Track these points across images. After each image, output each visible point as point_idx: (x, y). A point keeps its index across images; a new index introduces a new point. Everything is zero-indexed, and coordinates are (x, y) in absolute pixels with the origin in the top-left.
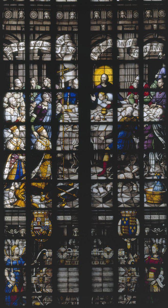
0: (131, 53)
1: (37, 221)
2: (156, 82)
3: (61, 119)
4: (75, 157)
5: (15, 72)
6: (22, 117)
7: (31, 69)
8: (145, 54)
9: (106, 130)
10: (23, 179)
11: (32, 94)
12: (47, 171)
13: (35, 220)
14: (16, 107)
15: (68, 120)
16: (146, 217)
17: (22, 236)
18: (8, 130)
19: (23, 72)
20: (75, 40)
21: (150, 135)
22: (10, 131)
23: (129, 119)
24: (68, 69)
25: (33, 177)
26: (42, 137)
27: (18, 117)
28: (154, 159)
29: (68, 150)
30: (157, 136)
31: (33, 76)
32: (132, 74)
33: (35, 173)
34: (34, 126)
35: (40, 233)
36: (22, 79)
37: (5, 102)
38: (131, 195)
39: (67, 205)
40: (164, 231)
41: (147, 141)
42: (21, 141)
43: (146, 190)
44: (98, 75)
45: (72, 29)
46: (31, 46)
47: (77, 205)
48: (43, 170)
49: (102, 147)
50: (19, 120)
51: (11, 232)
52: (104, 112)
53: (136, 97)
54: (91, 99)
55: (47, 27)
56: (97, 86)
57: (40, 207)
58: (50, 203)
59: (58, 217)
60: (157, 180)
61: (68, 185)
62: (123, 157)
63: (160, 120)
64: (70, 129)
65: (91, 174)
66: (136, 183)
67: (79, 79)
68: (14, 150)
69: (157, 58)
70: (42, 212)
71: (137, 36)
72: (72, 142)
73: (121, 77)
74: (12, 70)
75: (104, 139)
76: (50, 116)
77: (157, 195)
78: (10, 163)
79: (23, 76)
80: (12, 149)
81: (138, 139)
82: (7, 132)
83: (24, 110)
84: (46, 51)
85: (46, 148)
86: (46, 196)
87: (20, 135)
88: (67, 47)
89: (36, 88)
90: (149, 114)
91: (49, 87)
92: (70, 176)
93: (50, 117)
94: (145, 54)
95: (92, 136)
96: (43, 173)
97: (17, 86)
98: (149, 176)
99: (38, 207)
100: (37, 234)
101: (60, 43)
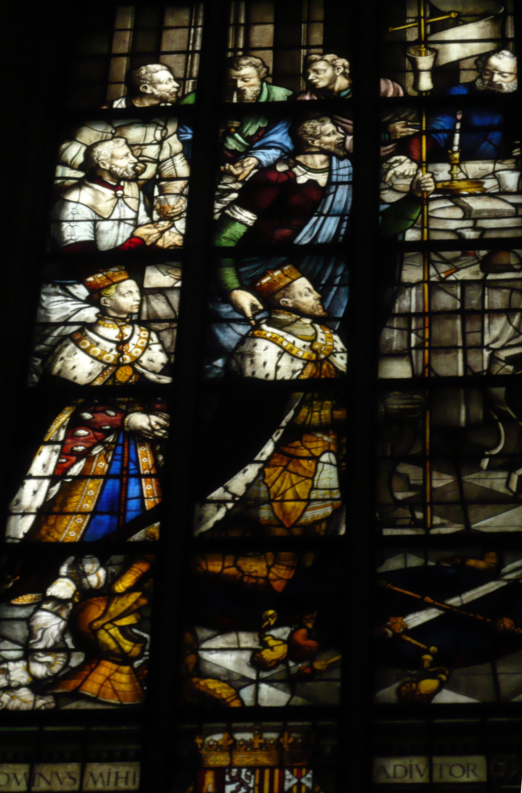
3: (412, 227)
6: (162, 223)
10: (139, 536)
12: (313, 488)
15: (454, 231)
18: (71, 289)
22: (81, 291)
25: (210, 524)
26: (283, 317)
27: (137, 226)
37: (65, 164)
39: (455, 688)
42: (149, 338)
50: (145, 238)
59: (380, 761)
68: (98, 383)
72: (482, 332)
74: (126, 30)
76: (341, 215)
78: (62, 454)
79: (186, 52)
83: (181, 194)
86: (303, 632)
87: (145, 308)
89: (259, 96)
91: (340, 91)
97: (149, 91)
99: (236, 704)
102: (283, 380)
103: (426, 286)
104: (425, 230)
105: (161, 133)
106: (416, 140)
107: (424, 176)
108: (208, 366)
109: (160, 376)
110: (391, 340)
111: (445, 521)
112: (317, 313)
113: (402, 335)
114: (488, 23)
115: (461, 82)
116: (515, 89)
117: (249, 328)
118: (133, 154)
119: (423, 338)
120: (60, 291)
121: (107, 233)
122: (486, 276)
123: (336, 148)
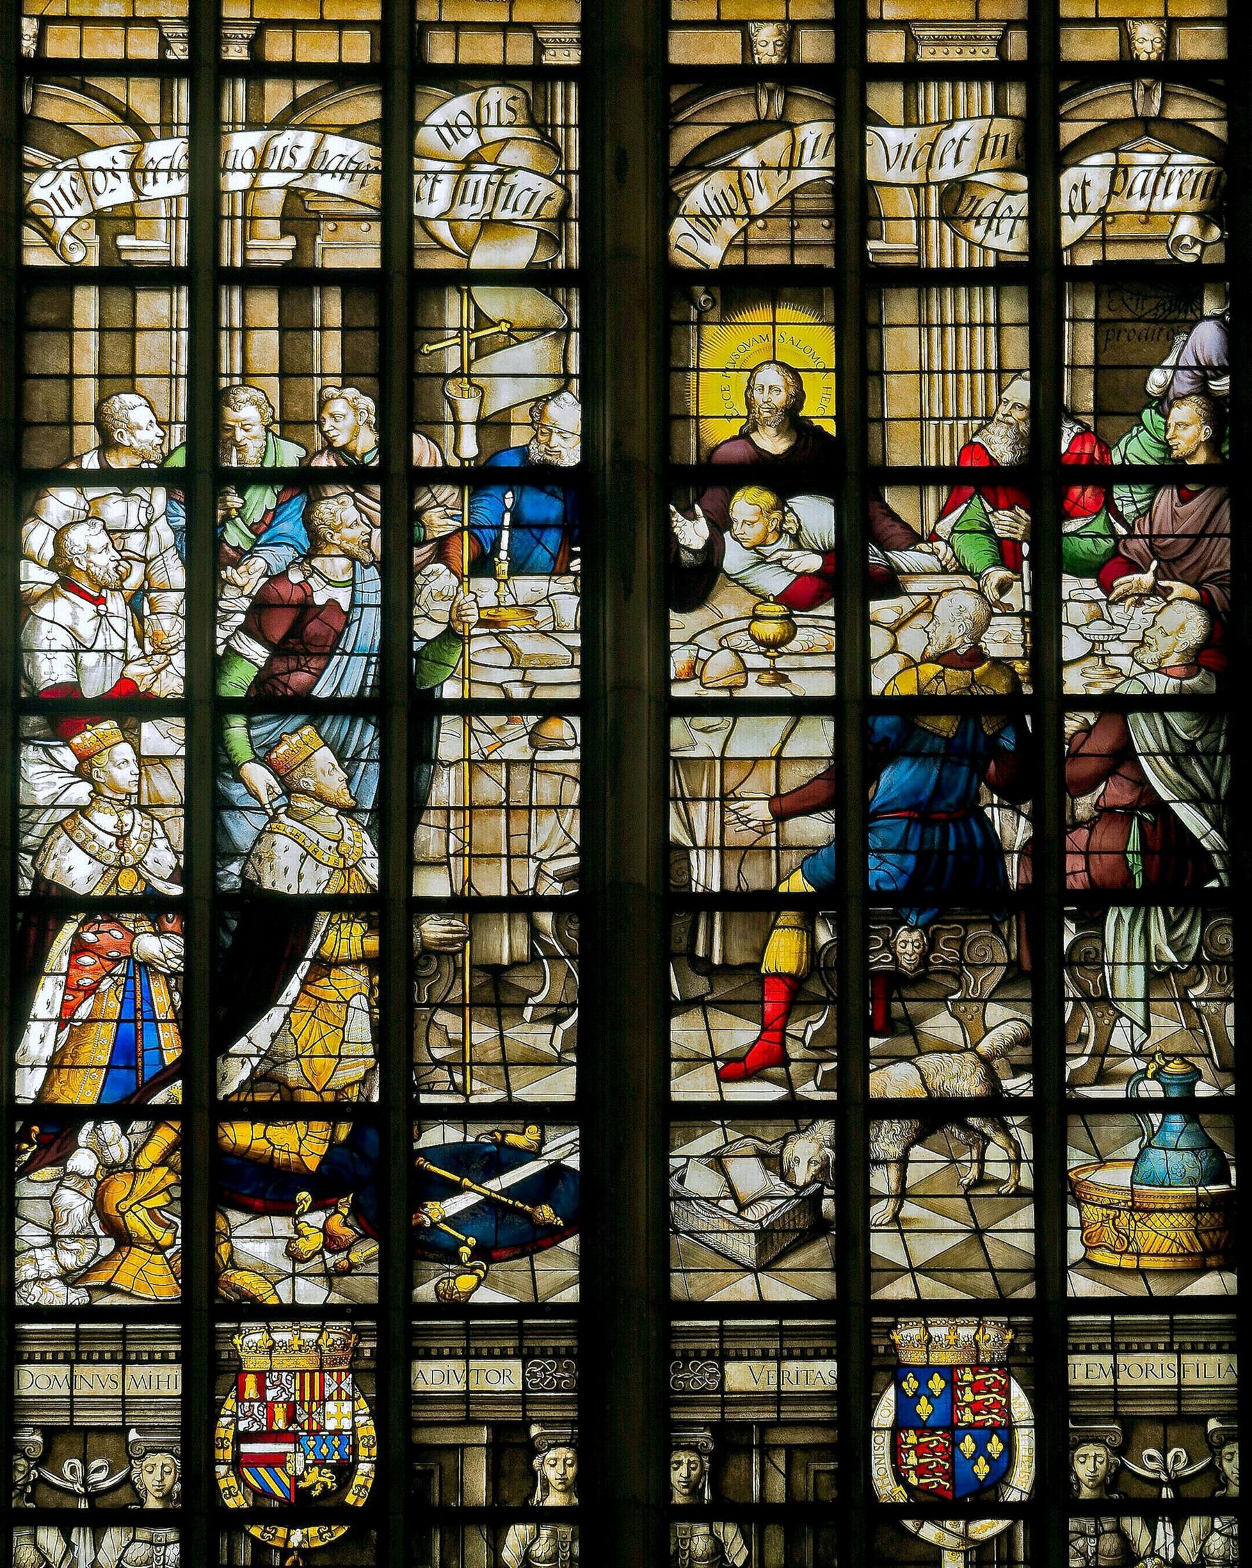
0: (967, 219)
1: (262, 1398)
2: (1157, 417)
4: (553, 942)
5: (108, 347)
6: (156, 657)
7: (231, 329)
10: (160, 1098)
12: (343, 1041)
13: (251, 1390)
15: (500, 685)
16: (1081, 1370)
17: (152, 1503)
19: (174, 348)
20: (554, 126)
21: (1115, 792)
22: (67, 757)
23: (955, 680)
24: (504, 327)
25: (234, 1086)
26: (304, 804)
28: (1138, 956)
29: (504, 893)
30: (1165, 794)
32: (979, 378)
33: (248, 1056)
34: (249, 726)
35: (287, 1482)
37: (30, 559)
38: (973, 1215)
39: (494, 1286)
40: (1213, 1471)
41: (1091, 830)
43: (1083, 1176)
45: (539, 47)
46: (234, 170)
47: (568, 1284)
49: (756, 877)
51: (68, 1475)
52: (769, 630)
54: (676, 536)
55: (349, 35)
56: (718, 447)
57: (287, 1300)
58: (362, 1270)
60: (1164, 1106)
61: (501, 1144)
62: (908, 943)
63: (1184, 682)
64: (517, 749)
65: (674, 1065)
66: (1005, 1129)
67: (585, 399)
68: (99, 892)
69: (1158, 253)
70: (305, 1336)
71: (1016, 100)
73: (892, 382)
75: (768, 816)
77: (1162, 1211)
78: (67, 988)
79: (170, 376)
80: (81, 889)
81: (1022, 819)
82: (46, 768)
87: (144, 787)
88: (496, 178)
90: (1102, 642)
91: (364, 455)
92: (512, 1077)
93: (369, 664)
95: (683, 799)
97: (126, 443)
98: (1103, 1078)
99: (273, 1301)
100: (262, 1493)
101: (448, 146)
103: (466, 764)
106: (456, 539)
107: (465, 599)
109: (170, 885)
110: (427, 842)
111: (485, 1086)
112: (343, 801)
115: (512, 446)
116: (578, 460)
122: (534, 754)
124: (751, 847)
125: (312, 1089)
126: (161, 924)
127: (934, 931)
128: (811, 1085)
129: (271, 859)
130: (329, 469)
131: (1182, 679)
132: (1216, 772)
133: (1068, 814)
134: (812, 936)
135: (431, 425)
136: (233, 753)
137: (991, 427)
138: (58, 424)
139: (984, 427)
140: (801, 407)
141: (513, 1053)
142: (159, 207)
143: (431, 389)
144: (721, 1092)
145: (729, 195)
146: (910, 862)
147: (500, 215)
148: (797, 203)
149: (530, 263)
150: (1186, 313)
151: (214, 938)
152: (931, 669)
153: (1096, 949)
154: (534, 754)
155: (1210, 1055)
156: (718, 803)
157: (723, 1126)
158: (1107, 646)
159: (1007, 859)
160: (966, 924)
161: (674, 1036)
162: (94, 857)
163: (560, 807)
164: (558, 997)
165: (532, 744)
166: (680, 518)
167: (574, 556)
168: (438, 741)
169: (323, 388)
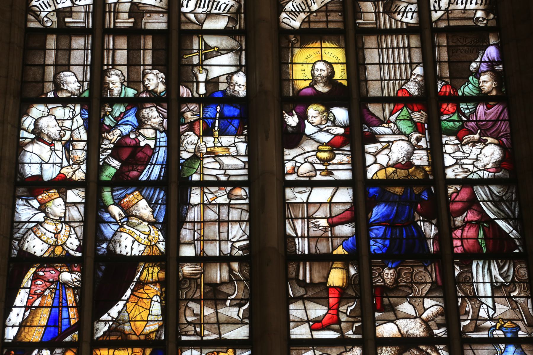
2: (475, 79)
3: (195, 173)
5: (59, 55)
6: (74, 166)
7: (108, 49)
8: (435, 16)
9: (333, 201)
10: (68, 339)
11: (109, 109)
12: (149, 315)
14: (57, 141)
15: (215, 176)
18: (30, 202)
19: (85, 57)
21: (471, 216)
22: (35, 204)
23: (402, 173)
24: (216, 49)
25: (101, 333)
26: (135, 221)
28: (487, 279)
29: (218, 255)
30: (492, 216)
31: (114, 65)
33: (108, 321)
34: (112, 191)
36: (82, 73)
37: (25, 130)
41: (463, 230)
42: (70, 231)
44: (303, 64)
48: (135, 311)
49: (323, 248)
52: (324, 155)
53: (416, 116)
54: (286, 122)
60: (506, 341)
62: (389, 274)
63: (496, 174)
64: (223, 200)
67: (247, 74)
68: (46, 255)
69: (470, 23)
73: (369, 67)
74: (52, 49)
75: (326, 224)
76: (162, 165)
78: (30, 294)
79: (84, 65)
80: (39, 254)
81: (433, 226)
83: (83, 150)
84: (155, 6)
85: (147, 248)
89: (120, 94)
90: (461, 159)
91: (161, 93)
93: (162, 168)
94: (435, 16)
95: (292, 218)
96: (135, 321)
97: (65, 88)
98: (478, 329)
102: (135, 256)
103: (202, 205)
104: (202, 174)
105: (72, 113)
106: (197, 123)
107: (201, 144)
108: (99, 247)
109: (76, 252)
110: (186, 235)
111: (210, 333)
112: (150, 219)
113: (191, 233)
114: (233, 55)
116: (245, 95)
117: (118, 226)
118: (58, 125)
119: (201, 235)
120: (25, 203)
121: (47, 171)
122: (230, 201)
123: (159, 126)
124: (321, 237)
125: (135, 334)
126: (72, 268)
127: (399, 269)
128: (350, 332)
129: (120, 242)
130: (146, 98)
131: (495, 173)
132: (513, 208)
133: (452, 224)
134: (348, 271)
135: (187, 83)
136: (105, 201)
137: (409, 83)
138: (38, 82)
139: (406, 83)
140: (333, 76)
141: (222, 319)
142: (81, 9)
143: (187, 71)
144: (312, 335)
145: (302, 5)
146: (387, 242)
147: (213, 11)
148: (328, 7)
149: (226, 27)
150: (483, 43)
151: (95, 273)
152: (391, 170)
153: (469, 277)
154: (230, 201)
155: (523, 320)
156: (306, 220)
157: (314, 349)
158: (463, 161)
159: (428, 241)
160: (413, 267)
161: (291, 312)
162: (45, 242)
163: (240, 221)
164: (241, 296)
165: (228, 197)
166: (287, 115)
167: (245, 129)
168: (190, 197)
169: (145, 69)
